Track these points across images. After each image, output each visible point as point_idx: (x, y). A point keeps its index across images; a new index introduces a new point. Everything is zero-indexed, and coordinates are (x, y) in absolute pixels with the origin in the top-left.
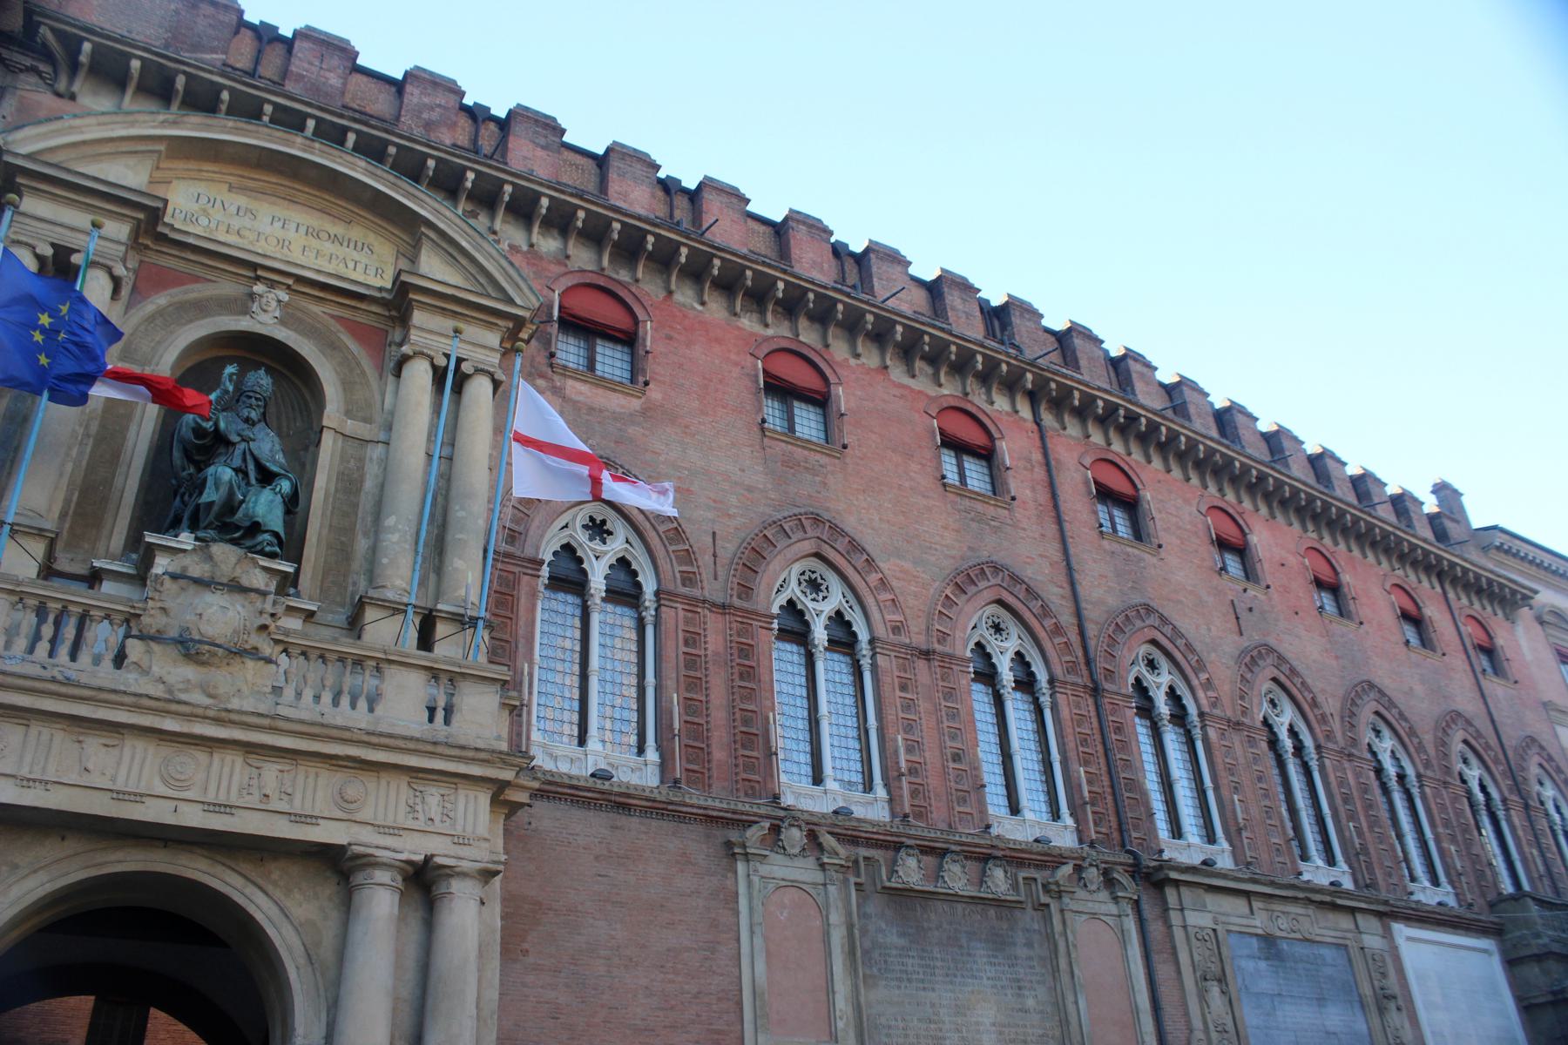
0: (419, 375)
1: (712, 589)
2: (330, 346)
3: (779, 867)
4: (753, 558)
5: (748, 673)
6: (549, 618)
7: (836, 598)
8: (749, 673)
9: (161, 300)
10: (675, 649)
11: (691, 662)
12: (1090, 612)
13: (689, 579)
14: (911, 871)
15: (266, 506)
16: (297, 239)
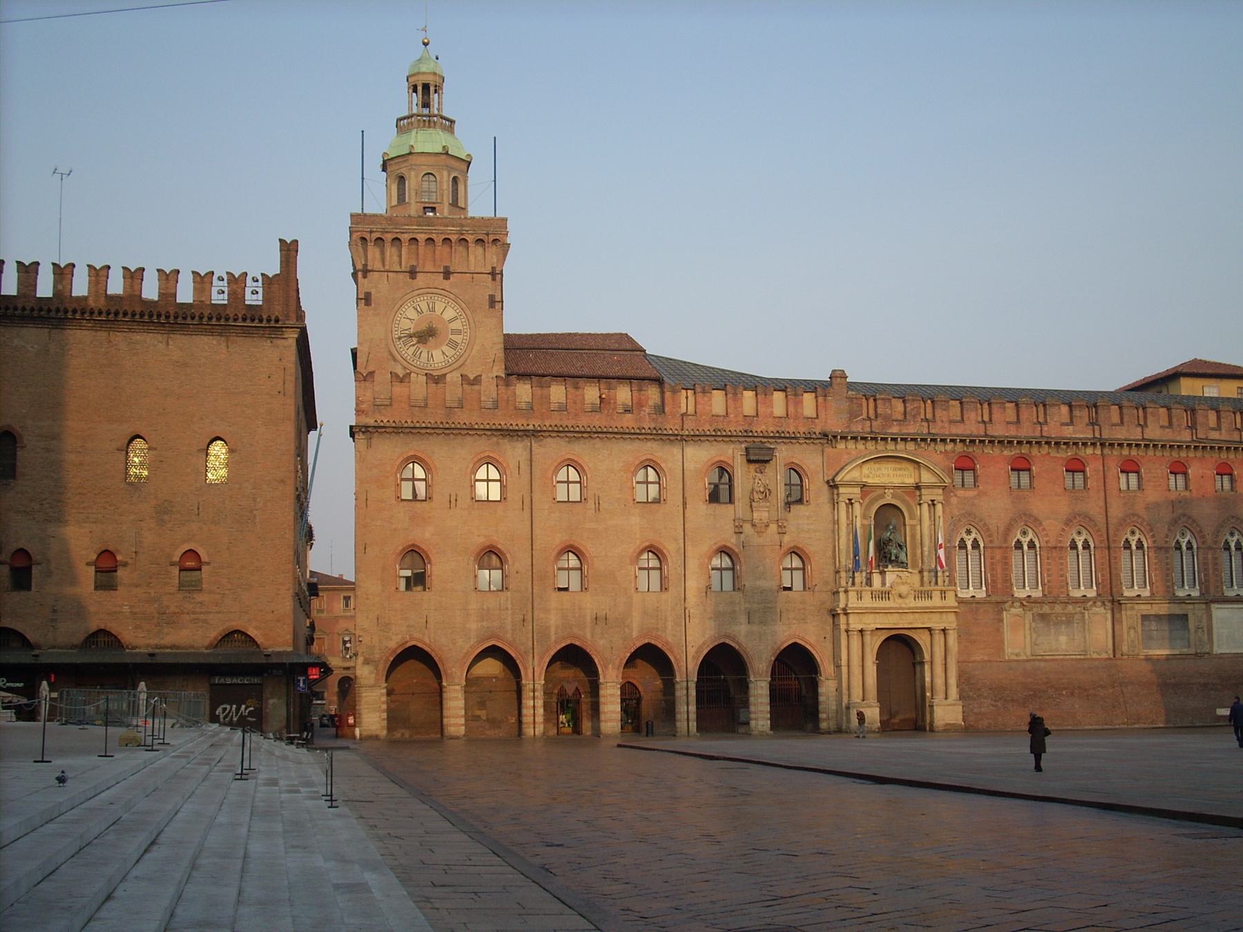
0: (925, 507)
1: (996, 543)
2: (903, 501)
3: (1013, 610)
4: (1008, 529)
5: (1006, 563)
6: (959, 557)
7: (1030, 535)
8: (1006, 563)
9: (867, 500)
10: (988, 561)
11: (992, 564)
12: (1112, 521)
13: (991, 542)
14: (1046, 609)
15: (902, 557)
16: (891, 472)
